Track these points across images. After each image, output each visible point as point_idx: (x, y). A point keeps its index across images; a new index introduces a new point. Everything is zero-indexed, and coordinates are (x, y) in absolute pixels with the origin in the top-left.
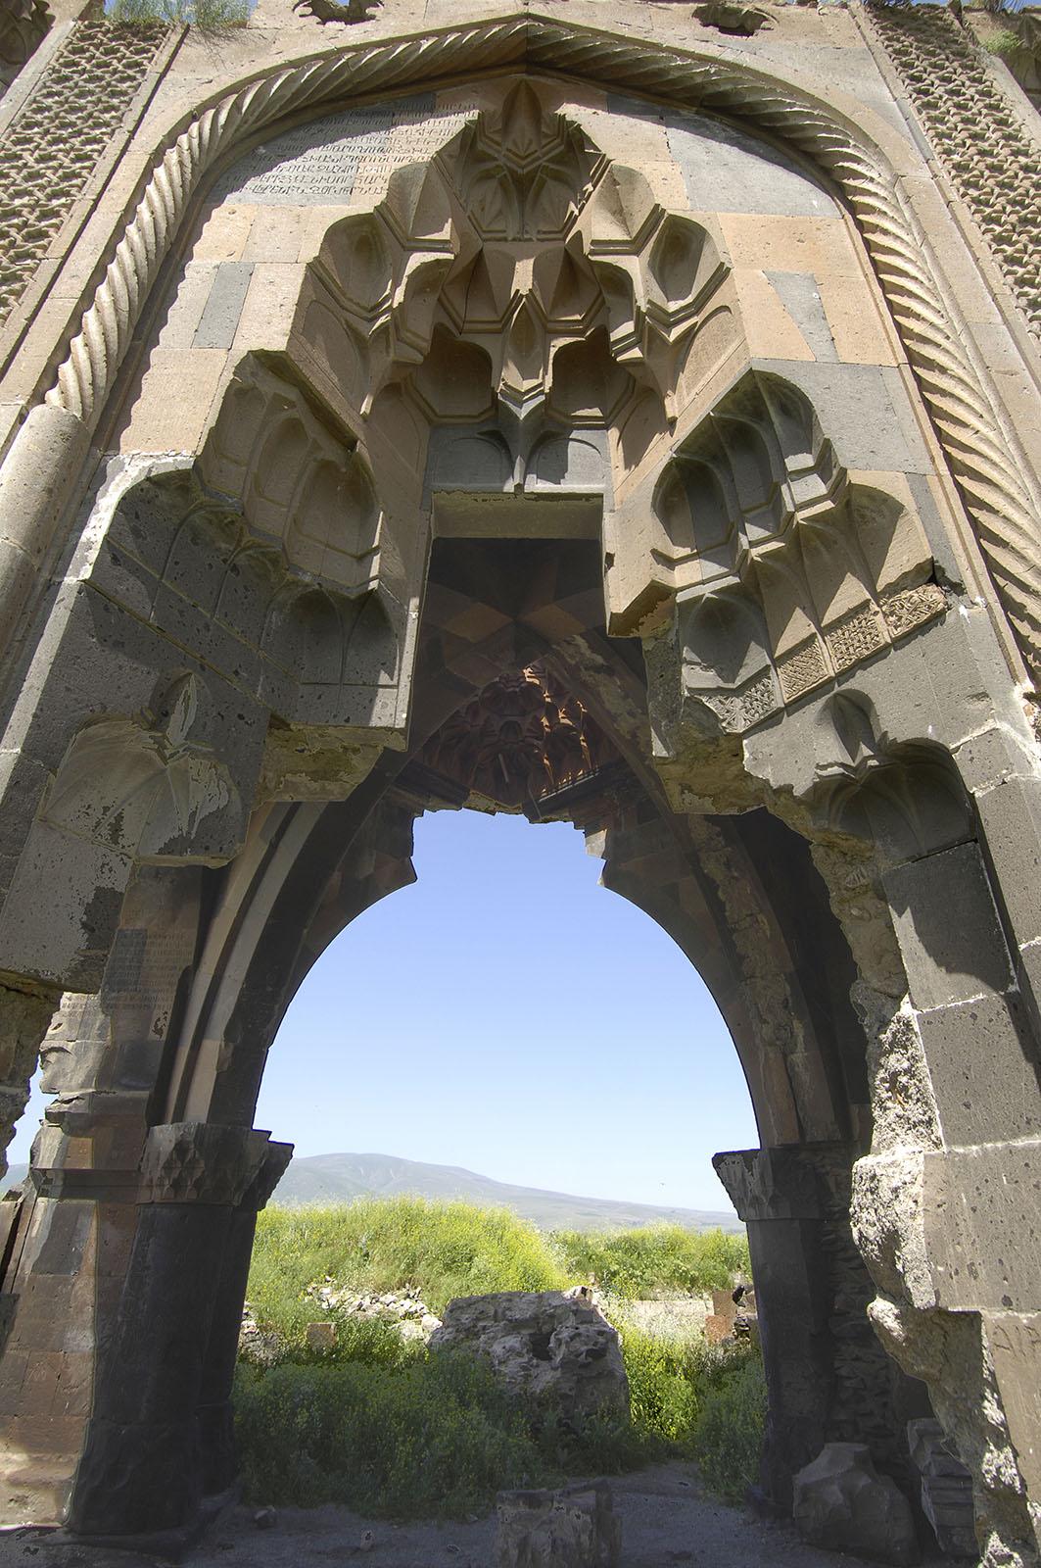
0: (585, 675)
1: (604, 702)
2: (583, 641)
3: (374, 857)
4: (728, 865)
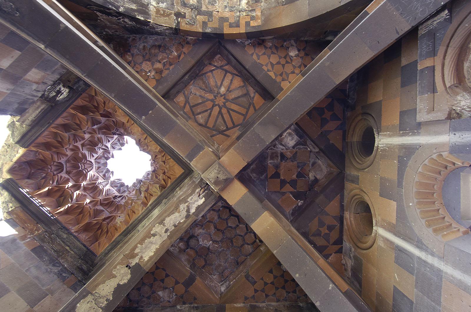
0: (183, 207)
1: (169, 217)
2: (202, 203)
3: (5, 91)
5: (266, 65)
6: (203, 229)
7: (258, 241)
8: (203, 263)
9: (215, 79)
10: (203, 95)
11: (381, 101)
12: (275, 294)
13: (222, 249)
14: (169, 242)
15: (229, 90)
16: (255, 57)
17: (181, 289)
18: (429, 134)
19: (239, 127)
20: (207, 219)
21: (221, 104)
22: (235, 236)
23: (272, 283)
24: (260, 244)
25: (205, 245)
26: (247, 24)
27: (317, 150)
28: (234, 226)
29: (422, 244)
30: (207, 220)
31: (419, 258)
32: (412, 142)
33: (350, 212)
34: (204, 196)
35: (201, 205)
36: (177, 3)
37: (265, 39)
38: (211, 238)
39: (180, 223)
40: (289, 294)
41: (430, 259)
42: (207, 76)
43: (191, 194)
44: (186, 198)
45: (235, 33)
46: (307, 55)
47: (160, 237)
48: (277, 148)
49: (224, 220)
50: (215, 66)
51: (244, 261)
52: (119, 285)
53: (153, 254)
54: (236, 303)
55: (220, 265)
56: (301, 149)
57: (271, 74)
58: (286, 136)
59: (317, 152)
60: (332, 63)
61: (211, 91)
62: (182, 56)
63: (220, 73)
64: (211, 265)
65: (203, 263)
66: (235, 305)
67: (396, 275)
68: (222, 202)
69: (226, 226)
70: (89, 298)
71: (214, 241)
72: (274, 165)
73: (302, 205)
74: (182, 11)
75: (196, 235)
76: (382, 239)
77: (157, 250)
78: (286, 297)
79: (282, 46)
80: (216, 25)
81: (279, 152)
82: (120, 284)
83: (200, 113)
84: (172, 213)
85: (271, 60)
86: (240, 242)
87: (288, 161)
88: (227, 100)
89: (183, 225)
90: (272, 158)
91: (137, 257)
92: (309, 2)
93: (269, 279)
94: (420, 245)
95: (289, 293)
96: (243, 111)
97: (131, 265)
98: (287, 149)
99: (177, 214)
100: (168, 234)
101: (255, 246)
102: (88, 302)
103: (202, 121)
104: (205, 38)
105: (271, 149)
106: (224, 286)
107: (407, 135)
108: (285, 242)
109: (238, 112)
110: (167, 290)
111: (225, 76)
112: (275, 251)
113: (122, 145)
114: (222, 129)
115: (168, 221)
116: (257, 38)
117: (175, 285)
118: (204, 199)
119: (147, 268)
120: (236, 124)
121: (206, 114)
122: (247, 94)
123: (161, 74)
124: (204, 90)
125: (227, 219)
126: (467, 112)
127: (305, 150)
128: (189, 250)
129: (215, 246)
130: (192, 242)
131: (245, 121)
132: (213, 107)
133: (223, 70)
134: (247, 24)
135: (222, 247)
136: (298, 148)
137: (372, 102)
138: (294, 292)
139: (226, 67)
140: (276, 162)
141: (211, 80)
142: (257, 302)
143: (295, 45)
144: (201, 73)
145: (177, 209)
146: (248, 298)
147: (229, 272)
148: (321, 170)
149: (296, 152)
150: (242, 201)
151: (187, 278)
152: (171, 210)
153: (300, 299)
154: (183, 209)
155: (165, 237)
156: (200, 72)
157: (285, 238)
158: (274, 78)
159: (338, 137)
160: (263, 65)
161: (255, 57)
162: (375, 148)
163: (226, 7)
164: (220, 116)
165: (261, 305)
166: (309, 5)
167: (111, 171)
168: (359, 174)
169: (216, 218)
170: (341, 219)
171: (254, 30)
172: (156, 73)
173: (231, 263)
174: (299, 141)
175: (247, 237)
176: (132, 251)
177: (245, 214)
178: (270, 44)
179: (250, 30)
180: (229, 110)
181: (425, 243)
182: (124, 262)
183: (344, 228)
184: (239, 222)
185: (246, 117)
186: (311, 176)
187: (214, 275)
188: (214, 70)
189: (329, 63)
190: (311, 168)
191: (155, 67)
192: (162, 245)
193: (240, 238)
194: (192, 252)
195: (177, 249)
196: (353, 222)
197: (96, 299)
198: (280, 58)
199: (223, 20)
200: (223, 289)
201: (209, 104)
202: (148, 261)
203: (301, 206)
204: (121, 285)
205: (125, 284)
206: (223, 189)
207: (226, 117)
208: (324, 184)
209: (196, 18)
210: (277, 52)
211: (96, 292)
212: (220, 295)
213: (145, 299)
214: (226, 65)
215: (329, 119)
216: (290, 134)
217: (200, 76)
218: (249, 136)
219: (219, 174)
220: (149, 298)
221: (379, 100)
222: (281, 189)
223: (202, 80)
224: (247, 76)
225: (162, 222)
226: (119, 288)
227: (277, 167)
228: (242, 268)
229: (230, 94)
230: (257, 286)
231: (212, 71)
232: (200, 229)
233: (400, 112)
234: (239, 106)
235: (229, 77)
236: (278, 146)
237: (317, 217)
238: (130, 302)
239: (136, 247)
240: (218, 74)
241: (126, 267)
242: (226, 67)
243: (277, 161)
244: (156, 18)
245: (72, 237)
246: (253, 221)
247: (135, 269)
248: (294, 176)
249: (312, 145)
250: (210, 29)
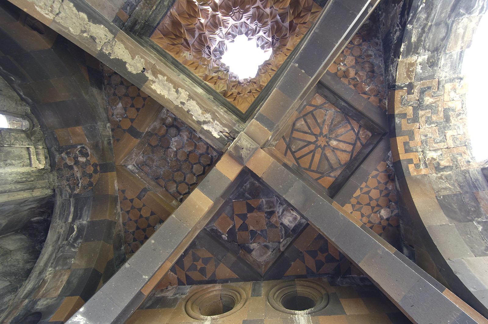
0: (208, 117)
1: (197, 104)
2: (214, 135)
4: (93, 38)
5: (367, 186)
6: (187, 140)
7: (181, 197)
8: (153, 144)
9: (345, 133)
10: (326, 123)
11: (344, 313)
12: (131, 220)
13: (170, 161)
14: (172, 107)
15: (334, 149)
16: (374, 173)
17: (126, 125)
19: (297, 165)
20: (198, 142)
21: (319, 143)
22: (184, 173)
23: (141, 216)
24: (179, 199)
25: (171, 143)
26: (410, 161)
27: (282, 249)
28: (194, 170)
30: (197, 143)
33: (221, 290)
34: (221, 137)
35: (212, 135)
36: (423, 84)
37: (395, 181)
38: (179, 149)
39: (192, 115)
40: (132, 235)
42: (347, 125)
43: (221, 123)
44: (218, 119)
45: (399, 148)
46: (384, 228)
47: (175, 98)
48: (279, 207)
49: (199, 160)
50: (359, 132)
51: (160, 185)
52: (125, 63)
53: (159, 92)
54: (117, 182)
55: (153, 161)
56: (281, 232)
57: (358, 193)
58: (293, 214)
59: (279, 249)
60: (381, 257)
61: (331, 131)
62: (365, 96)
63: (352, 138)
64: (153, 152)
65: (153, 144)
66: (116, 181)
68: (217, 156)
69: (193, 163)
70: (110, 36)
71: (176, 153)
72: (260, 205)
73: (223, 239)
74: (415, 91)
75: (181, 133)
77: (162, 97)
78: (128, 232)
79: (390, 201)
80: (404, 128)
81: (275, 209)
82: (126, 64)
83: (306, 122)
84: (201, 107)
85: (373, 191)
86: (178, 179)
87: (267, 219)
88: (323, 149)
89: (190, 119)
90: (267, 202)
91: (154, 78)
92: (444, 225)
93: (145, 213)
95: (133, 235)
96: (314, 167)
97: (145, 73)
98: (279, 217)
99: (200, 112)
100: (179, 106)
101: (176, 194)
102: (106, 35)
103: (298, 125)
104: (389, 117)
105: (277, 201)
106: (134, 168)
108: (185, 225)
109: (313, 161)
110: (124, 111)
111: (349, 143)
113: (263, 47)
114: (293, 148)
115: (192, 104)
116: (396, 174)
117: (130, 119)
118: (219, 137)
119: (144, 89)
120: (299, 161)
121: (306, 129)
122: (332, 169)
123: (343, 77)
124: (332, 123)
125: (199, 163)
127: (281, 237)
128: (165, 128)
129: (171, 154)
130: (173, 131)
131: (304, 170)
132: (315, 135)
133: (356, 141)
134: (410, 161)
135: (171, 161)
136: (282, 229)
137: (342, 304)
138: (135, 240)
139: (359, 144)
140: (265, 207)
141: (343, 130)
142: (121, 203)
143: (393, 214)
144: (348, 117)
145: (205, 111)
146: (124, 193)
147: (147, 171)
148: (261, 256)
149: (277, 227)
150: (221, 176)
151: (138, 130)
152: (204, 105)
153: (128, 247)
154: (206, 117)
155: (176, 103)
156: (350, 116)
157: (188, 225)
158: (354, 195)
159: (298, 270)
160: (366, 182)
161: (374, 173)
162: (293, 311)
163: (426, 136)
164: (306, 144)
165: (118, 207)
166: (441, 225)
167: (234, 39)
168: (263, 297)
169: (200, 152)
170: (213, 281)
171: (404, 169)
172: (344, 72)
173: (157, 172)
174: (289, 229)
175: (184, 185)
176: (159, 71)
177: (208, 181)
178: (390, 187)
179: (404, 164)
180: (313, 152)
182: (148, 65)
183: (204, 285)
184: (198, 176)
185: (307, 170)
186: (254, 246)
187: (143, 157)
188: (354, 131)
189: (381, 254)
190: (262, 244)
191: (350, 69)
192: (169, 101)
193: (182, 179)
194: (163, 131)
195: (165, 116)
196: (211, 294)
197: (109, 43)
198: (377, 200)
199: (411, 135)
200: (130, 167)
201: (317, 131)
202: (151, 89)
203: (222, 237)
204: (125, 66)
205: (126, 69)
206: (231, 155)
207: (306, 150)
209: (409, 106)
210: (383, 196)
211: (116, 42)
212: (124, 165)
213: (113, 90)
214: (361, 143)
215: (317, 258)
216: (295, 219)
217: (346, 118)
218: (289, 176)
219: (247, 149)
220: (114, 94)
221: (345, 311)
222: (237, 215)
223: (342, 120)
224: (353, 166)
225: (190, 97)
226: (122, 64)
227: (259, 209)
228: (153, 184)
229: (331, 151)
230: (136, 201)
231: (353, 129)
232: (187, 136)
234: (319, 162)
235: (349, 148)
236: (281, 207)
237: (212, 256)
238: (109, 76)
239: (164, 75)
240: (351, 136)
241: (144, 68)
242: (359, 144)
243: (265, 208)
244: (404, 64)
245: (165, 11)
246: (202, 190)
247: (142, 77)
248: (251, 228)
249: (287, 243)
250: (399, 122)
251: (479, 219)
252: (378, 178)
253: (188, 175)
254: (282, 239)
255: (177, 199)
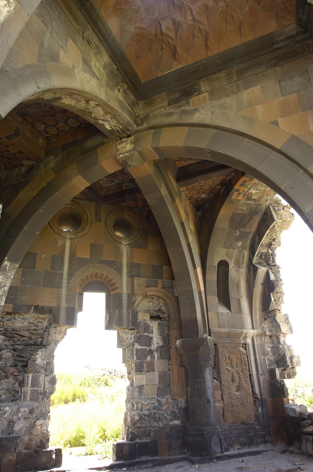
7: (48, 135)
13: (43, 106)
18: (127, 283)
24: (45, 136)
27: (124, 188)
28: (69, 122)
29: (72, 276)
31: (63, 275)
32: (124, 272)
33: (71, 205)
35: (105, 127)
37: (223, 186)
41: (65, 281)
57: (197, 184)
59: (122, 186)
67: (45, 255)
76: (63, 244)
79: (212, 192)
94: (70, 275)
107: (127, 268)
112: (58, 193)
118: (110, 129)
126: (134, 299)
134: (238, 190)
157: (67, 199)
158: (192, 185)
160: (206, 181)
161: (215, 179)
166: (222, 228)
178: (218, 187)
181: (72, 278)
198: (204, 190)
208: (94, 187)
210: (210, 190)
233: (140, 264)
249: (129, 186)
251: (242, 230)
252: (215, 182)
253: (61, 123)
254: (126, 180)
255: (43, 136)
